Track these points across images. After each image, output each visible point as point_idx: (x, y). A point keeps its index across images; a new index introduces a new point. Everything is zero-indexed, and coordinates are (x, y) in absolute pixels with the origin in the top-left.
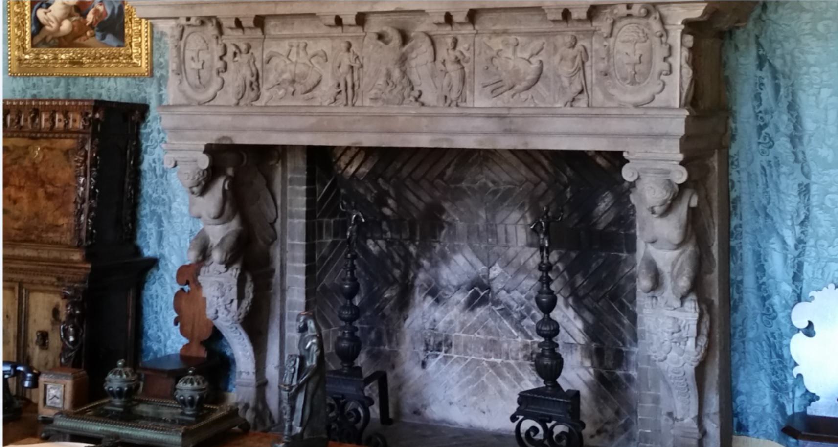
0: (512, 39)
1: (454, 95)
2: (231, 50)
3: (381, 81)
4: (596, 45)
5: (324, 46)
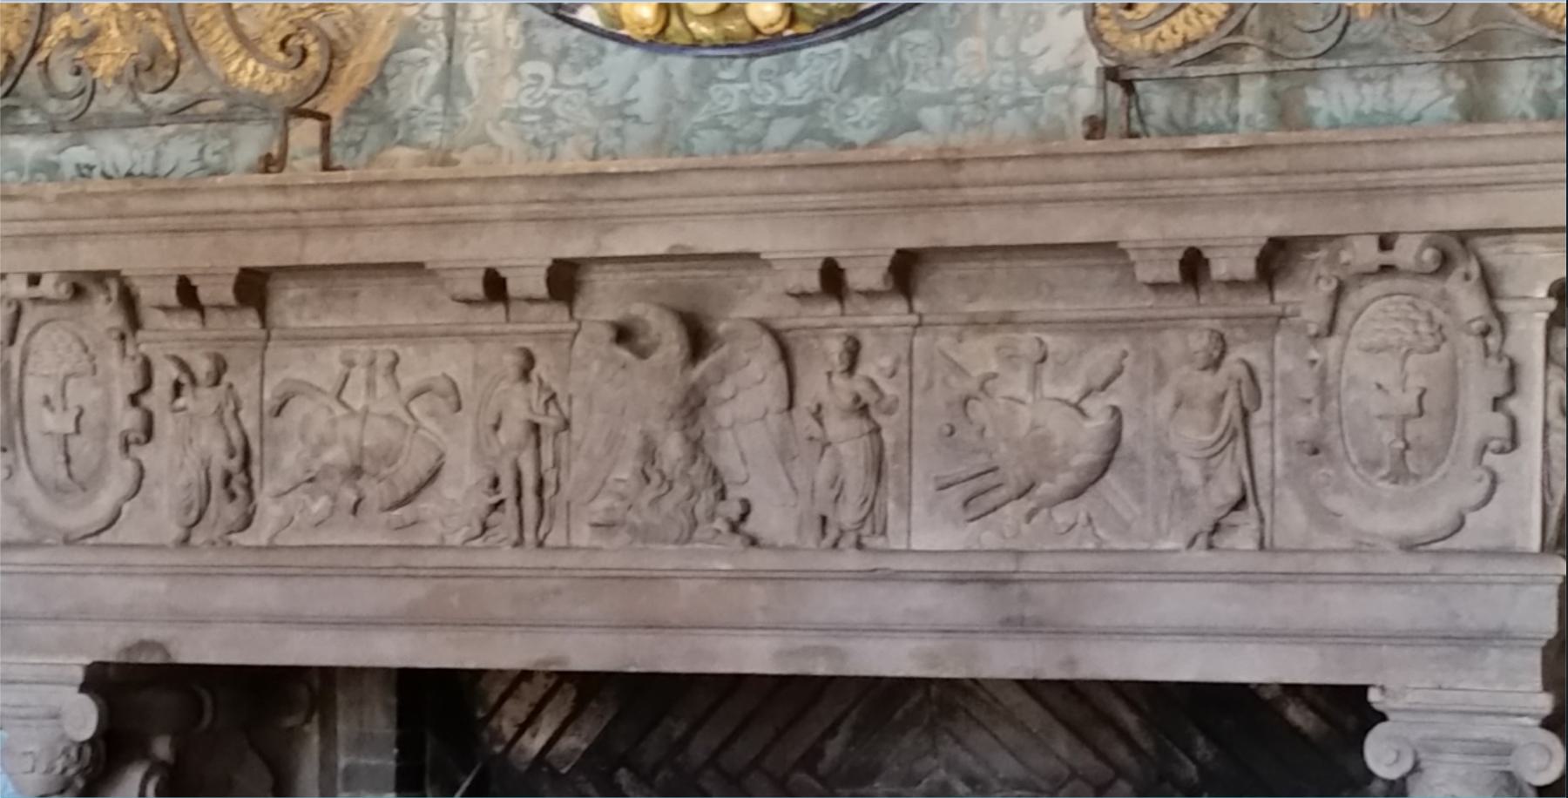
0: (1026, 342)
1: (848, 515)
2: (165, 374)
3: (625, 472)
4: (1285, 361)
5: (450, 362)
